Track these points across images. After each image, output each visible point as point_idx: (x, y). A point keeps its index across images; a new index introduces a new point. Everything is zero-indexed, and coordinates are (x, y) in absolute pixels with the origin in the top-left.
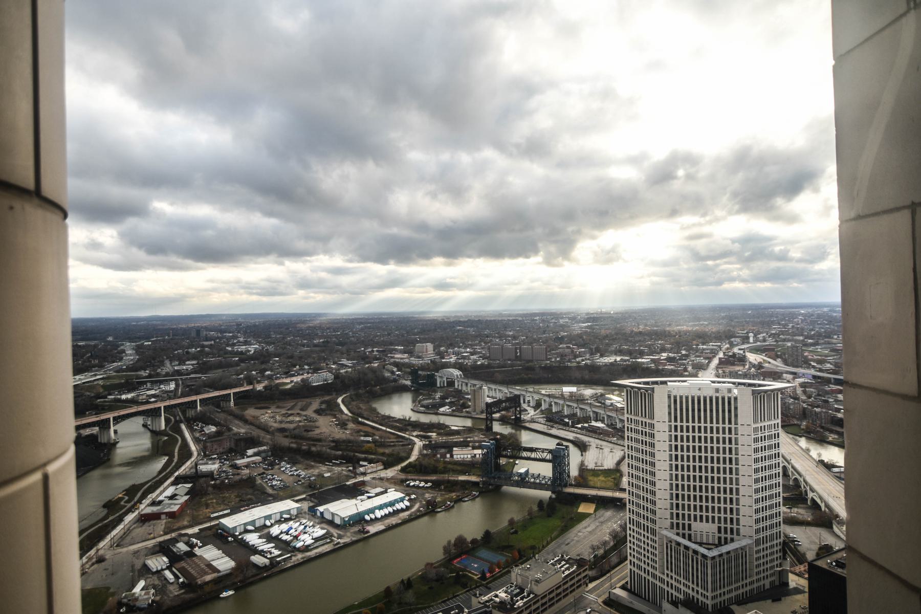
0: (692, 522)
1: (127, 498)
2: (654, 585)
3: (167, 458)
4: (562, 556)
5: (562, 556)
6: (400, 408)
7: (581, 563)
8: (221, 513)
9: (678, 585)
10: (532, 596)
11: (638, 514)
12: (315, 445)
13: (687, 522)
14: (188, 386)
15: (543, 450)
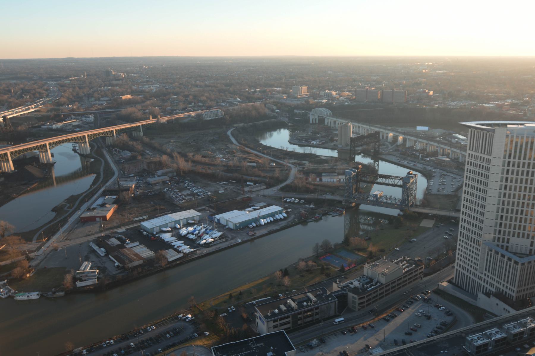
0: (511, 237)
1: (68, 205)
2: (474, 281)
3: (95, 175)
4: (404, 258)
5: (404, 258)
6: (279, 139)
7: (418, 263)
8: (141, 218)
9: (492, 282)
10: (378, 284)
11: (468, 230)
12: (209, 169)
13: (506, 237)
14: (105, 119)
15: (396, 178)
